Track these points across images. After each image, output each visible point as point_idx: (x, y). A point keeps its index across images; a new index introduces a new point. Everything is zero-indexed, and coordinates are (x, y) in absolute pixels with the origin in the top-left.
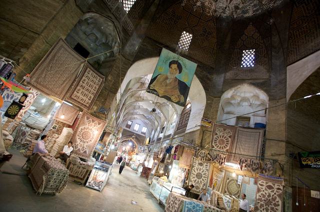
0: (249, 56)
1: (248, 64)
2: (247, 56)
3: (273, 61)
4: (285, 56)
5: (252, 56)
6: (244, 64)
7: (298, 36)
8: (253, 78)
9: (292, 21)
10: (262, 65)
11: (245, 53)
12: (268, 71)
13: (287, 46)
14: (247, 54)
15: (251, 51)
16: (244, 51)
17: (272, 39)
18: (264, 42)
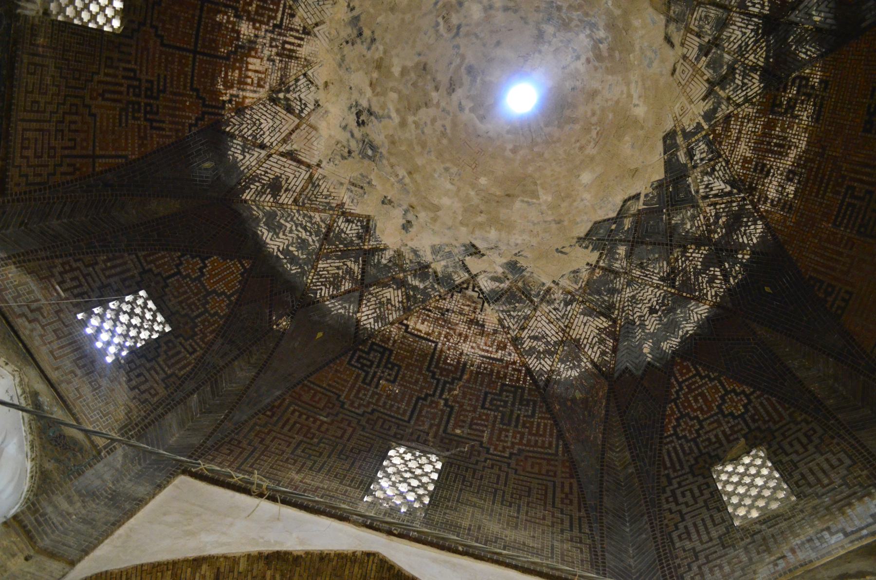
0: (136, 321)
1: (105, 336)
2: (131, 314)
3: (169, 416)
4: (209, 443)
5: (144, 335)
6: (95, 322)
7: (287, 427)
8: (63, 388)
9: (311, 379)
10: (132, 389)
11: (140, 302)
12: (124, 430)
13: (245, 417)
14: (138, 311)
15: (160, 318)
16: (142, 293)
17: (236, 363)
18: (211, 343)
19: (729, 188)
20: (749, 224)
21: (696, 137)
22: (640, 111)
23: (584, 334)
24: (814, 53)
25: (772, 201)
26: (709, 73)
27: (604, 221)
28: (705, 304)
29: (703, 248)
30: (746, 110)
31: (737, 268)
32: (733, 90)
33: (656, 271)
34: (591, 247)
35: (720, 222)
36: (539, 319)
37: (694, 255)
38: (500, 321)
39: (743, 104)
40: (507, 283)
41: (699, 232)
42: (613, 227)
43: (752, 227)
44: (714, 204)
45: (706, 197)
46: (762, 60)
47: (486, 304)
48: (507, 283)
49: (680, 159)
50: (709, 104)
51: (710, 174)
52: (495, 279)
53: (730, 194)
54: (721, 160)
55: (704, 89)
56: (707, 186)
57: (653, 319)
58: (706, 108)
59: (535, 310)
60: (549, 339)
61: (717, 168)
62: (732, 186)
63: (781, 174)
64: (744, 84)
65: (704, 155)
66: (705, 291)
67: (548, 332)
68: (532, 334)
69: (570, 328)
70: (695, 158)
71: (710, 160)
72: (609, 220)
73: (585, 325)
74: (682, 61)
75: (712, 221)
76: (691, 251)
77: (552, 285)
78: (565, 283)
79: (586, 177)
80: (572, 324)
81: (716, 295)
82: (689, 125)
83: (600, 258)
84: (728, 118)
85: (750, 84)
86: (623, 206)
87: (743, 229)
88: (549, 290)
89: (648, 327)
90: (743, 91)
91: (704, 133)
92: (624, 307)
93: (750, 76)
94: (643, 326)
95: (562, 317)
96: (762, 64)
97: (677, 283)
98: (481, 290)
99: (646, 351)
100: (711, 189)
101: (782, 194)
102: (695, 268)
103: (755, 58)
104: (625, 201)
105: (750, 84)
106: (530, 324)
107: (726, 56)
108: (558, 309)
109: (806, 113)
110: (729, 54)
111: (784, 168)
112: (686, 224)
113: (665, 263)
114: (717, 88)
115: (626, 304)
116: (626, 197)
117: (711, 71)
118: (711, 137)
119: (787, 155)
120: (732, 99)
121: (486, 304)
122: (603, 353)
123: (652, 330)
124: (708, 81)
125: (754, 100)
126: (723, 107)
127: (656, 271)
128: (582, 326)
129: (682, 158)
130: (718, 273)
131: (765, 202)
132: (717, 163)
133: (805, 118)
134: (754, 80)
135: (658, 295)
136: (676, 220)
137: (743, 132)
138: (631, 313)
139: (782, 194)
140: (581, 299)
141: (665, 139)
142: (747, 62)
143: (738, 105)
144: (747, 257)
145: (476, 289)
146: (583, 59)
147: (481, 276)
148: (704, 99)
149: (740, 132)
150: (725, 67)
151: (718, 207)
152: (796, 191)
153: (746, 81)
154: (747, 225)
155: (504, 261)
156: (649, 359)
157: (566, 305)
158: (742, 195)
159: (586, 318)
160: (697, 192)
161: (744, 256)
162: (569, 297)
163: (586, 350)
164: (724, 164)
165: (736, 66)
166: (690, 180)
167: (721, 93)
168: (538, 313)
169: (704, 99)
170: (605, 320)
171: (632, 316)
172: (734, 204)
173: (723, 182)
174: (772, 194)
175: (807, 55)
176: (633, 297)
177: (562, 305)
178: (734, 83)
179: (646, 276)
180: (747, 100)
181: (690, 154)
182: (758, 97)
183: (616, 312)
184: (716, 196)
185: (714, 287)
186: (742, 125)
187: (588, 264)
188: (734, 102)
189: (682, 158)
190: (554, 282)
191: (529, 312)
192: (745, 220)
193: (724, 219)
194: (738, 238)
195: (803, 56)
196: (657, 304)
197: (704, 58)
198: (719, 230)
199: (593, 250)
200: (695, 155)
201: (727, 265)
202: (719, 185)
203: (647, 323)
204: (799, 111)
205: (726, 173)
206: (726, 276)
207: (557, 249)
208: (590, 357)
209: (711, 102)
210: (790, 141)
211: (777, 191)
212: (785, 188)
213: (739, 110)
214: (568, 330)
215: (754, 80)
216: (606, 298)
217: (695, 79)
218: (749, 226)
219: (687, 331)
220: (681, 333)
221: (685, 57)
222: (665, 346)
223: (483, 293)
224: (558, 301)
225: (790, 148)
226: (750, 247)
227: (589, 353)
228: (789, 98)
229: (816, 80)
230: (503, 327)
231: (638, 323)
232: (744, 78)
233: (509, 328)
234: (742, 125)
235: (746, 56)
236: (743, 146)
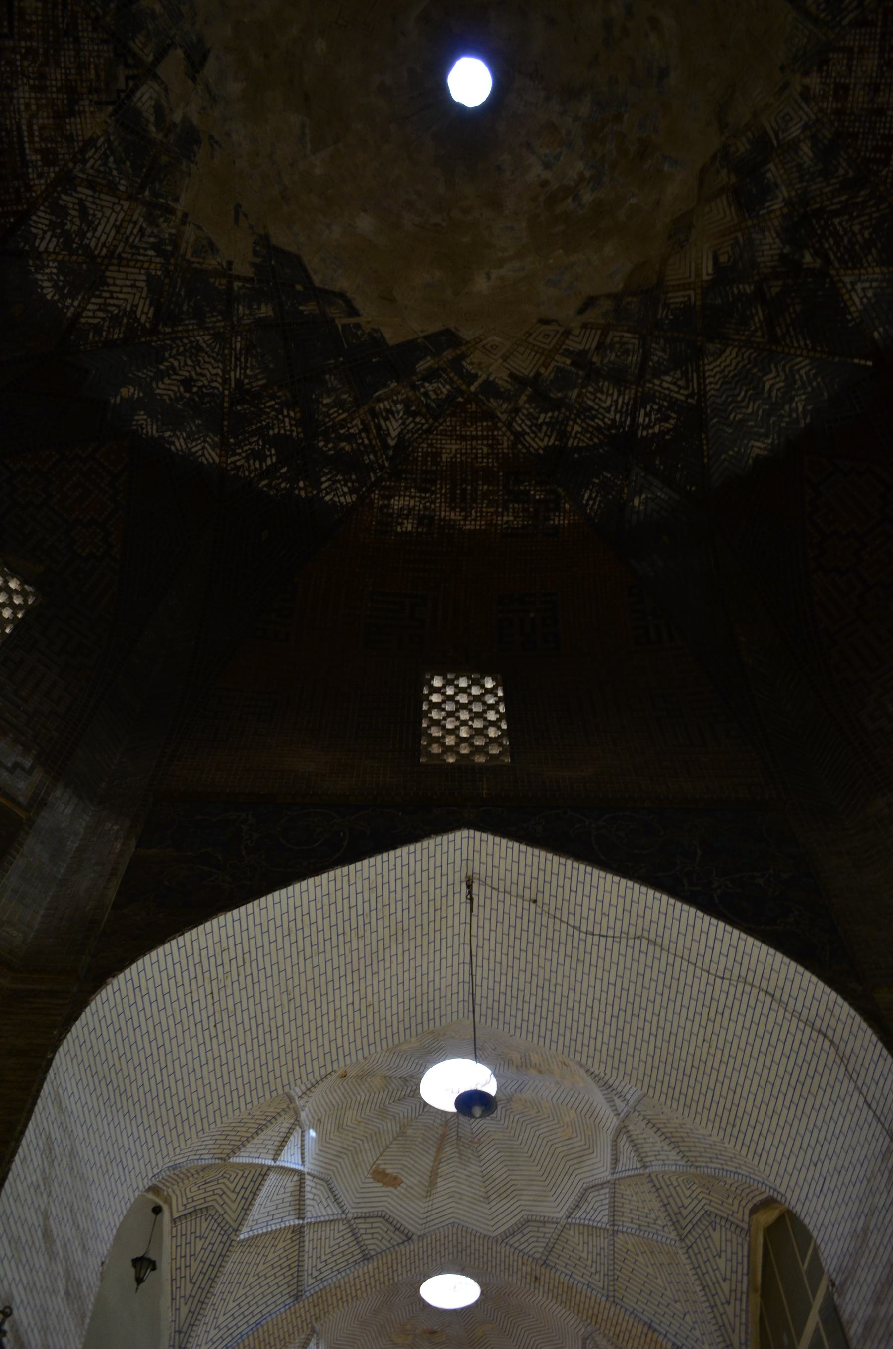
19: (392, 443)
20: (349, 485)
21: (456, 378)
22: (481, 285)
23: (117, 289)
24: (591, 509)
25: (388, 506)
26: (547, 373)
27: (305, 270)
28: (220, 456)
29: (300, 430)
30: (505, 438)
31: (283, 485)
32: (530, 414)
33: (248, 372)
34: (258, 260)
35: (343, 444)
36: (117, 208)
37: (287, 420)
38: (91, 142)
39: (512, 433)
40: (160, 136)
41: (321, 418)
42: (299, 287)
43: (346, 490)
44: (366, 429)
45: (374, 414)
46: (575, 444)
47: (110, 108)
48: (160, 136)
49: (421, 363)
50: (505, 385)
51: (408, 412)
52: (159, 110)
53: (386, 446)
54: (430, 421)
55: (526, 372)
56: (389, 411)
57: (175, 388)
58: (500, 382)
59: (130, 198)
60: (89, 235)
61: (418, 420)
62: (396, 446)
63: (425, 508)
64: (540, 428)
65: (433, 396)
66: (239, 451)
67: (100, 229)
68: (88, 205)
69: (119, 265)
70: (426, 384)
71: (427, 406)
72: (308, 277)
73: (133, 286)
74: (561, 330)
75: (342, 431)
76: (292, 414)
77: (179, 214)
78: (190, 234)
79: (365, 223)
80: (128, 266)
81: (237, 468)
82: (472, 363)
83: (246, 280)
84: (490, 416)
85: (541, 435)
86: (334, 293)
87: (340, 477)
88: (172, 212)
89: (161, 385)
90: (530, 427)
91: (464, 387)
92: (180, 339)
93: (552, 432)
94: (160, 376)
95: (132, 246)
96: (569, 444)
97: (239, 408)
98: (133, 92)
99: (124, 391)
100: (386, 419)
101: (399, 516)
102: (268, 427)
103: (577, 432)
104: (342, 295)
105: (541, 435)
106: (103, 196)
107: (576, 392)
108: (143, 235)
109: (511, 518)
110: (579, 396)
111: (434, 510)
112: (329, 397)
113: (263, 382)
114: (529, 390)
115: (185, 341)
116: (349, 295)
117: (552, 375)
118: (461, 399)
119: (453, 509)
120: (517, 415)
121: (110, 108)
122: (97, 329)
123: (158, 391)
124: (538, 374)
125: (520, 446)
126: (505, 406)
127: (248, 372)
128: (128, 283)
129: (423, 365)
130: (269, 462)
131: (383, 497)
132: (424, 417)
133: (505, 518)
134: (546, 439)
135: (214, 384)
136: (332, 380)
137: (474, 443)
138: (174, 352)
139: (399, 516)
140: (171, 268)
141: (447, 332)
142: (571, 423)
143: (509, 426)
144: (303, 494)
145: (131, 84)
146: (547, 175)
147: (156, 87)
148: (511, 375)
149: (474, 438)
150: (559, 395)
151: (363, 435)
152: (407, 533)
153: (544, 428)
154: (344, 480)
155: (195, 121)
156: (112, 400)
157: (153, 247)
158: (387, 464)
159: (143, 284)
160: (379, 400)
161: (302, 489)
162: (169, 248)
163: (93, 300)
164: (426, 426)
165: (563, 410)
166: (394, 385)
167: (524, 398)
168: (126, 204)
169: (511, 375)
170: (150, 315)
171: (171, 356)
172: (372, 456)
173: (400, 433)
174: (397, 503)
175: (588, 501)
176: (200, 349)
177: (152, 240)
178: (540, 413)
179: (237, 359)
180: (519, 436)
181: (431, 375)
182: (524, 450)
183: (168, 330)
184: (378, 427)
185: (247, 461)
186: (483, 438)
187: (230, 263)
188: (514, 419)
189: (423, 365)
190: (185, 215)
191: (122, 188)
192: (354, 477)
193: (348, 448)
194: (326, 474)
195: (586, 496)
196: (200, 388)
197: (568, 362)
198: (330, 445)
199: (253, 264)
200: (430, 383)
201: (284, 470)
202: (394, 427)
203: (167, 381)
204: (514, 508)
205: (413, 434)
206: (269, 473)
207: (238, 207)
208: (85, 309)
209: (509, 387)
210: (472, 508)
211: (402, 509)
212: (407, 518)
213: (504, 429)
214: (115, 261)
215: (546, 439)
216: (185, 308)
217: (538, 356)
218: (346, 485)
219: (173, 443)
220: (168, 434)
221: (567, 333)
222: (141, 417)
223: (128, 97)
224: (155, 231)
225: (462, 510)
226: (318, 494)
227: (90, 307)
228: (530, 491)
229: (557, 520)
230: (83, 151)
231: (162, 367)
232: (547, 424)
233: (85, 161)
234: (483, 438)
235: (579, 421)
236: (454, 447)
